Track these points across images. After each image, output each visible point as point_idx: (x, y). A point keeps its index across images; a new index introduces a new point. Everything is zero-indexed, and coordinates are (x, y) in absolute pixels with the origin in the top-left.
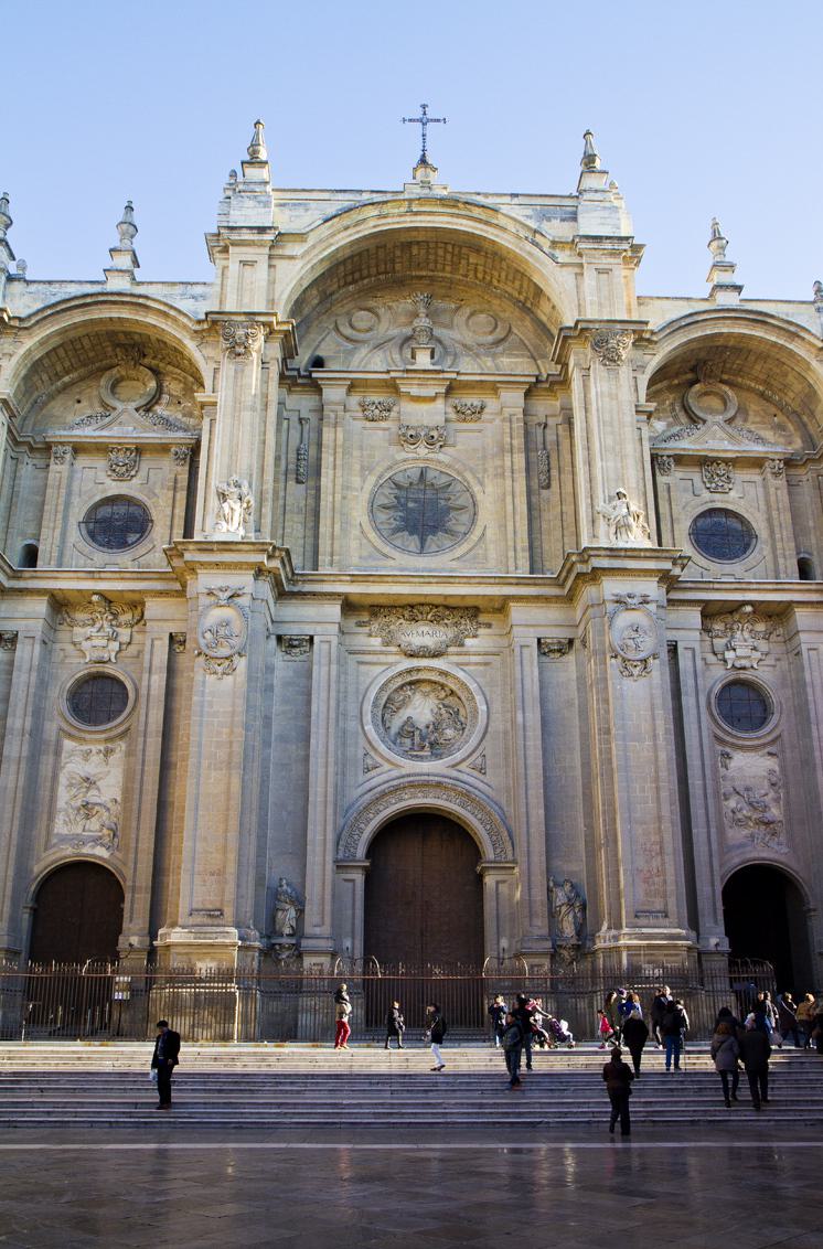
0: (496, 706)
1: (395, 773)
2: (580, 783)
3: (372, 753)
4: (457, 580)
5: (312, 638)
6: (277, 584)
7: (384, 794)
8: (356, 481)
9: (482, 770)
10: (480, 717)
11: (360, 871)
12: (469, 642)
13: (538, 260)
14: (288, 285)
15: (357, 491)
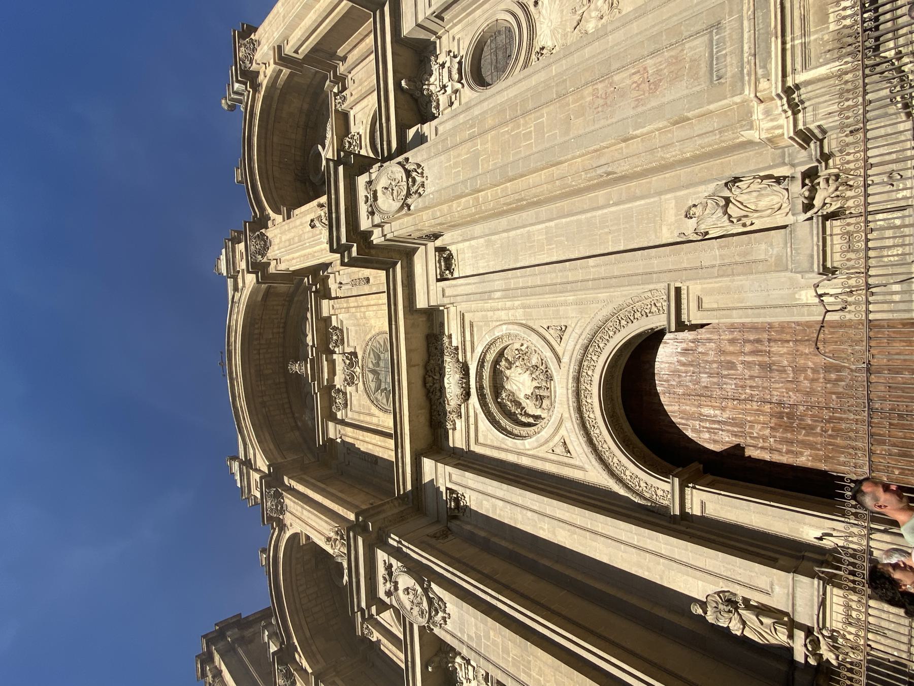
0: (503, 315)
1: (568, 424)
2: (564, 220)
3: (551, 444)
4: (395, 357)
5: (447, 489)
6: (401, 518)
7: (590, 442)
8: (375, 420)
9: (563, 330)
10: (512, 332)
11: (688, 491)
12: (454, 344)
13: (245, 299)
14: (264, 461)
15: (379, 420)
